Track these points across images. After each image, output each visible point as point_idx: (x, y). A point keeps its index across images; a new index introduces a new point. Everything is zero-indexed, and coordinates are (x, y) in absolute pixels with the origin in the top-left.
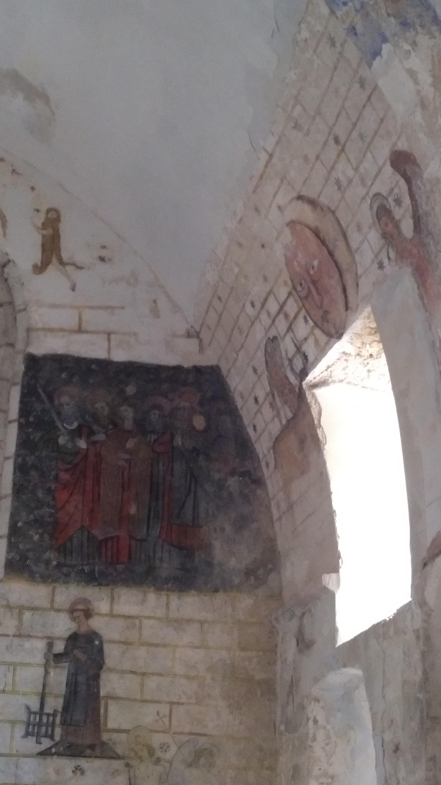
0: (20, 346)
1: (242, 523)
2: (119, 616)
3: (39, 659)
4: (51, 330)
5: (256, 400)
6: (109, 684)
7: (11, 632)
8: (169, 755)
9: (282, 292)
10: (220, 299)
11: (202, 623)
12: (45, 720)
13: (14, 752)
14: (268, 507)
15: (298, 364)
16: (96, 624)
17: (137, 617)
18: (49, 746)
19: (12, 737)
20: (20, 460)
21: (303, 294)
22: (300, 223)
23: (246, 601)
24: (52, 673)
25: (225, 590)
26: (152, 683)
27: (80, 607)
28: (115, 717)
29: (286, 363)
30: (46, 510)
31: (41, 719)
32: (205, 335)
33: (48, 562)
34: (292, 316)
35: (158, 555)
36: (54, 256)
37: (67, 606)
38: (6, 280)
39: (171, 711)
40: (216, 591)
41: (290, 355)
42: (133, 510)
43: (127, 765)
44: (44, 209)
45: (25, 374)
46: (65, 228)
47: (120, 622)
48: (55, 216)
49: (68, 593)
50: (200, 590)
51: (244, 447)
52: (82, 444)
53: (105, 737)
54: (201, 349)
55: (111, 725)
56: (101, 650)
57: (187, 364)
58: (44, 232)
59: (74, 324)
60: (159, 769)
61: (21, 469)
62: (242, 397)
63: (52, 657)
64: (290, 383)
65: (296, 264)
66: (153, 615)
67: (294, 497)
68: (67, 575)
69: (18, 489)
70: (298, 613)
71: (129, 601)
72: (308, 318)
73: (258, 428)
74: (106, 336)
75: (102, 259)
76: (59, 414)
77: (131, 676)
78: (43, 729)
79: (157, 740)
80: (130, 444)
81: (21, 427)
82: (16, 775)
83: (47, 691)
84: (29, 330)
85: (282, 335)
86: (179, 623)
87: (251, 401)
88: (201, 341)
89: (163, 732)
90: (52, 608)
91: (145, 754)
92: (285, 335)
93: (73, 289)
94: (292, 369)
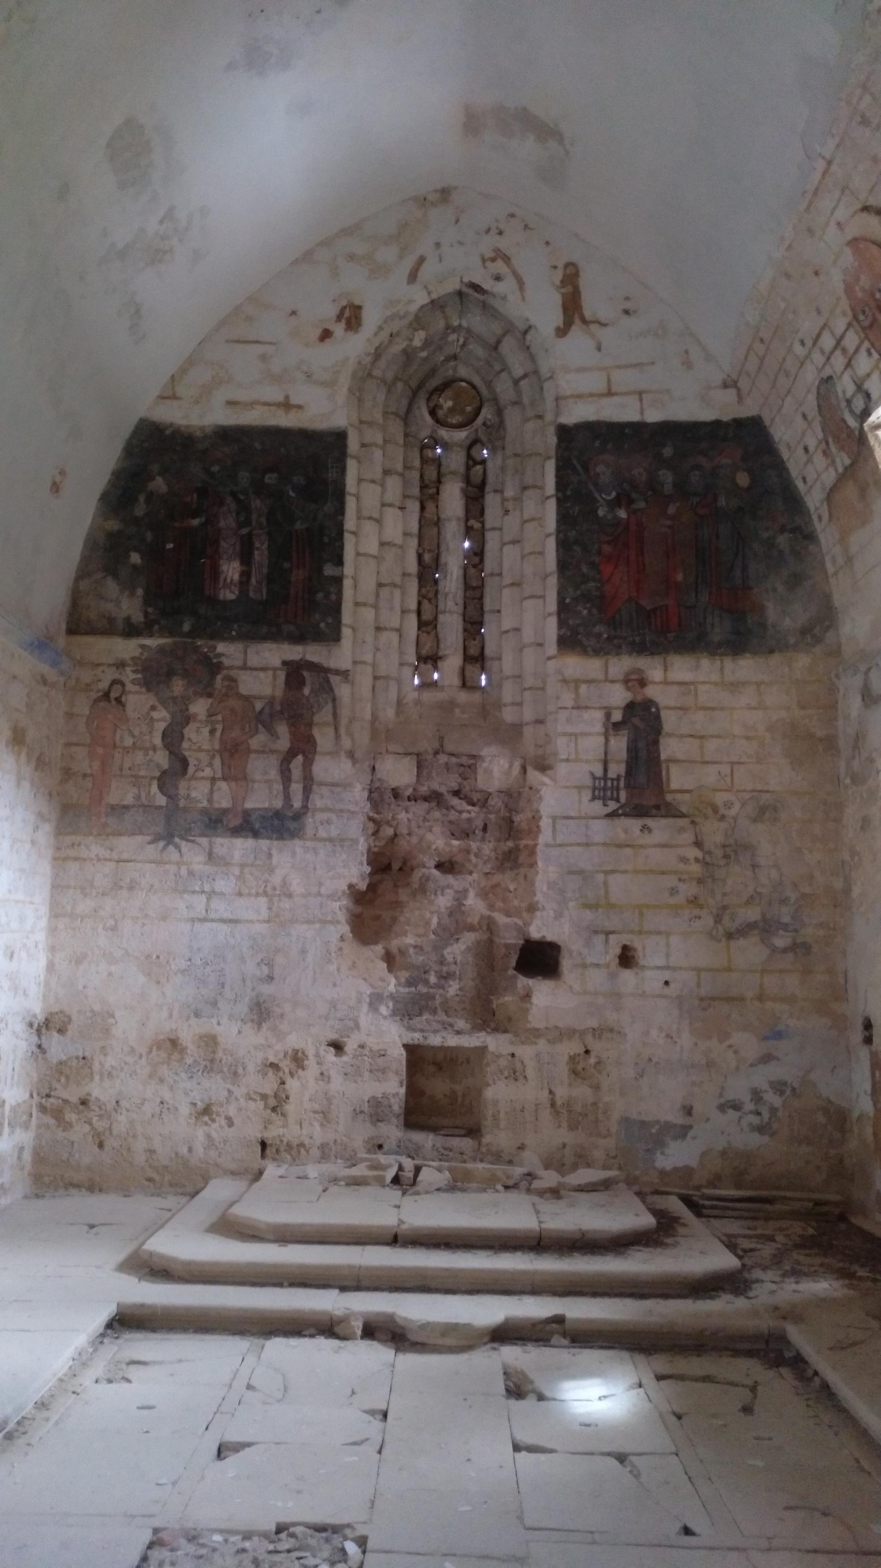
0: (549, 417)
1: (796, 580)
2: (673, 683)
3: (599, 728)
4: (580, 396)
5: (806, 449)
6: (669, 748)
7: (570, 704)
8: (733, 812)
9: (840, 325)
10: (762, 341)
11: (758, 684)
12: (609, 784)
13: (583, 815)
14: (823, 563)
15: (859, 404)
16: (651, 692)
17: (692, 683)
18: (616, 808)
19: (580, 802)
20: (561, 535)
21: (867, 323)
22: (865, 239)
23: (802, 661)
24: (612, 741)
25: (781, 651)
26: (711, 745)
27: (634, 677)
28: (677, 779)
29: (843, 404)
30: (592, 585)
31: (605, 784)
32: (744, 384)
33: (599, 635)
34: (851, 351)
35: (709, 620)
36: (576, 315)
37: (621, 677)
38: (528, 348)
39: (732, 770)
40: (771, 652)
41: (849, 394)
42: (680, 577)
43: (693, 822)
44: (561, 265)
45: (558, 446)
46: (584, 282)
48: (574, 271)
49: (622, 664)
50: (755, 653)
51: (794, 502)
52: (622, 514)
53: (669, 797)
55: (674, 786)
56: (658, 717)
57: (725, 419)
58: (563, 290)
59: (602, 387)
60: (724, 825)
61: (563, 545)
62: (789, 448)
63: (611, 725)
64: (848, 427)
65: (857, 288)
66: (707, 680)
67: (854, 549)
68: (619, 647)
69: (562, 566)
70: (863, 668)
71: (682, 668)
72: (873, 351)
73: (808, 479)
74: (637, 396)
75: (627, 312)
76: (596, 485)
77: (691, 739)
78: (609, 793)
79: (720, 798)
80: (672, 510)
81: (559, 502)
82: (587, 836)
83: (609, 758)
84: (557, 399)
85: (839, 372)
86: (735, 687)
87: (800, 451)
88: (739, 390)
89: (726, 790)
90: (606, 680)
91: (709, 811)
92: (843, 373)
93: (599, 349)
94: (852, 412)
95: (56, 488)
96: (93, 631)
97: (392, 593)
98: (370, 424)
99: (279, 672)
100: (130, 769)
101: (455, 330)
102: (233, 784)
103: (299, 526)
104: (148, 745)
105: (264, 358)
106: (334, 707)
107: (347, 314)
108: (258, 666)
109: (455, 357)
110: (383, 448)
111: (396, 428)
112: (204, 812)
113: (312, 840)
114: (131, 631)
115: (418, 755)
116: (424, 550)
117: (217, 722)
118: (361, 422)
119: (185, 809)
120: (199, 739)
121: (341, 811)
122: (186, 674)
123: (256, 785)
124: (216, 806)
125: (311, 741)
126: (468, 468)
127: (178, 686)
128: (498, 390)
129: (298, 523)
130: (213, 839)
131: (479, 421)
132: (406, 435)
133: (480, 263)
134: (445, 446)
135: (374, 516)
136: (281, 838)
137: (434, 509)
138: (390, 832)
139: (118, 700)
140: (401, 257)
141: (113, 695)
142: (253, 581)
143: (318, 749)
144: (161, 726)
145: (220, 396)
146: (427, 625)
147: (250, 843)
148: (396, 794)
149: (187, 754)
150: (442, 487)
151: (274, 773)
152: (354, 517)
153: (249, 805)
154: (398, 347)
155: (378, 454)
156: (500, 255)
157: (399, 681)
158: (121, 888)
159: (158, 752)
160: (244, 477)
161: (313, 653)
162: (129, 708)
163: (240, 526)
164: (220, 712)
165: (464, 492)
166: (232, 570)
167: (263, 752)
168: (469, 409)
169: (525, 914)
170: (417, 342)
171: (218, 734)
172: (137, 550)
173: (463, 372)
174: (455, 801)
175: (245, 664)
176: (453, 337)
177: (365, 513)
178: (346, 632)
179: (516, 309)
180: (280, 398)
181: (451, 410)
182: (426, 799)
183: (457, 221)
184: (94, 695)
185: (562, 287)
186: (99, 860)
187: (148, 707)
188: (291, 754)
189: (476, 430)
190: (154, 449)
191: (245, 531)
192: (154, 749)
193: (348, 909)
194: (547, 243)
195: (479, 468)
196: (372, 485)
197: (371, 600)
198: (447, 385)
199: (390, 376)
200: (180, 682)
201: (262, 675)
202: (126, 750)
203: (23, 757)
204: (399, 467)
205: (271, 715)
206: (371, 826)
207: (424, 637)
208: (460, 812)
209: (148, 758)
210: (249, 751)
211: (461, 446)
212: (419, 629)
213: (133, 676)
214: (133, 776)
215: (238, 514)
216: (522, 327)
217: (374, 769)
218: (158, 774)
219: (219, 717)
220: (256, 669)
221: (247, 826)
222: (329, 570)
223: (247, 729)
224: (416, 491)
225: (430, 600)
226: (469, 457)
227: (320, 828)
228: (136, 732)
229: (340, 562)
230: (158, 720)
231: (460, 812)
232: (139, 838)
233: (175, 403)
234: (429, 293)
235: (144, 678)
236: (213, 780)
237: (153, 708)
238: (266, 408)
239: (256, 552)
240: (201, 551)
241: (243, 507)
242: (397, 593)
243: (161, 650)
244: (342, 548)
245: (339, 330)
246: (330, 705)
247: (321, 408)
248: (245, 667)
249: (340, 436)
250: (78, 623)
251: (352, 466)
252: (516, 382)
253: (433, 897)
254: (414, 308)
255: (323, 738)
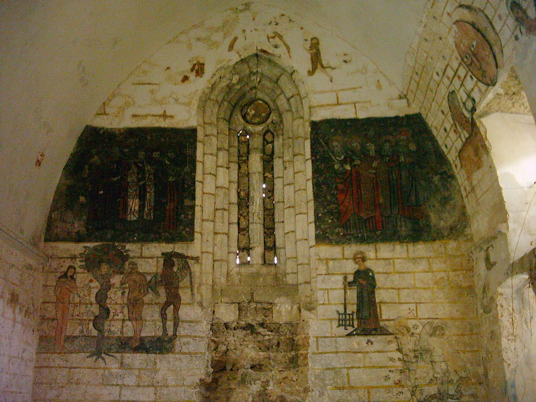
0: (306, 117)
1: (445, 201)
2: (381, 259)
3: (340, 285)
4: (322, 106)
5: (445, 130)
6: (380, 295)
7: (324, 272)
8: (418, 331)
9: (455, 64)
10: (417, 73)
11: (428, 258)
12: (348, 317)
13: (334, 335)
14: (459, 191)
15: (470, 105)
16: (369, 264)
17: (391, 259)
18: (352, 331)
19: (332, 328)
20: (315, 180)
21: (469, 63)
22: (462, 21)
23: (452, 245)
24: (348, 292)
25: (440, 240)
26: (404, 293)
27: (359, 256)
28: (386, 313)
29: (462, 105)
30: (332, 206)
31: (346, 317)
32: (410, 96)
33: (338, 234)
34: (462, 77)
35: (399, 224)
36: (319, 64)
37: (352, 257)
38: (294, 82)
39: (416, 307)
40: (434, 240)
41: (464, 100)
42: (381, 201)
43: (396, 338)
44: (309, 39)
45: (311, 132)
46: (322, 47)
47: (383, 262)
48: (316, 42)
49: (351, 249)
50: (425, 241)
51: (441, 158)
52: (348, 167)
53: (382, 324)
54: (409, 105)
55: (384, 317)
56: (373, 278)
58: (311, 52)
59: (335, 101)
60: (413, 338)
61: (316, 185)
63: (347, 284)
64: (465, 117)
65: (462, 45)
66: (400, 256)
67: (475, 182)
68: (350, 240)
69: (316, 196)
70: (485, 247)
71: (385, 250)
72: (473, 77)
73: (448, 146)
74: (353, 105)
75: (345, 62)
76: (333, 152)
77: (392, 290)
78: (348, 322)
79: (411, 323)
80: (375, 164)
81: (313, 162)
82: (336, 347)
83: (347, 302)
84: (310, 108)
85: (458, 89)
86: (415, 260)
87: (442, 131)
88: (408, 100)
89: (414, 319)
90: (344, 258)
91: (405, 331)
92: (460, 89)
93: (331, 81)
94: (466, 108)
95: (39, 163)
96: (58, 239)
97: (223, 214)
98: (210, 124)
99: (160, 259)
100: (78, 315)
101: (254, 74)
102: (134, 323)
103: (171, 179)
104: (88, 302)
105: (152, 92)
106: (191, 278)
107: (196, 67)
108: (148, 256)
109: (255, 88)
110: (217, 137)
111: (224, 126)
112: (119, 338)
113: (178, 353)
114: (79, 239)
115: (239, 303)
116: (241, 190)
117: (126, 288)
118: (205, 123)
119: (108, 338)
120: (116, 298)
121: (195, 337)
122: (109, 262)
123: (147, 323)
124: (125, 335)
125: (177, 297)
126: (264, 146)
127: (105, 268)
128: (279, 104)
129: (171, 178)
130: (124, 355)
131: (269, 120)
132: (230, 129)
133: (267, 39)
134: (251, 134)
135: (213, 173)
136: (161, 353)
137: (246, 168)
138: (224, 348)
139: (72, 277)
140: (225, 38)
141: (69, 275)
142: (146, 209)
143: (182, 302)
144: (95, 291)
145: (129, 112)
146: (243, 230)
147: (144, 356)
148: (227, 326)
149: (109, 306)
150: (250, 157)
151: (157, 316)
152: (201, 174)
153: (143, 334)
154: (224, 83)
155: (214, 139)
156: (277, 35)
157: (228, 262)
158: (72, 383)
159: (93, 306)
160: (141, 154)
161: (179, 248)
162: (78, 280)
163: (139, 180)
164: (127, 282)
165: (262, 159)
166: (134, 204)
167: (152, 304)
168: (264, 114)
169: (302, 394)
170: (234, 81)
171: (126, 294)
172: (83, 195)
173: (260, 95)
174: (261, 330)
175: (141, 255)
176: (253, 78)
177: (207, 171)
178: (197, 236)
179: (285, 61)
180: (161, 112)
181: (254, 116)
182: (244, 329)
183: (254, 19)
184: (59, 275)
185: (311, 50)
186: (60, 367)
187: (88, 280)
188: (167, 304)
189: (268, 126)
190: (93, 140)
191: (142, 183)
192: (91, 304)
193: (200, 393)
194: (302, 28)
195: (270, 145)
196: (211, 157)
197: (211, 218)
198: (252, 102)
199: (220, 98)
200: (106, 267)
201: (151, 261)
202: (76, 305)
203: (17, 311)
204: (226, 146)
205: (156, 283)
206: (213, 345)
207: (241, 237)
208: (264, 336)
209: (88, 309)
210: (143, 303)
211: (260, 135)
212: (239, 233)
213: (80, 264)
214: (80, 320)
215: (138, 174)
216: (290, 71)
217: (214, 312)
218: (93, 318)
219: (127, 285)
220: (147, 258)
221: (143, 346)
222: (187, 202)
223: (142, 292)
224: (236, 159)
225: (244, 217)
226: (264, 139)
227: (184, 347)
228: (81, 295)
229: (194, 198)
230: (94, 288)
231: (264, 336)
232: (83, 355)
233: (105, 117)
234: (240, 56)
235: (86, 264)
236: (124, 320)
237: (91, 281)
238: (154, 118)
239: (148, 194)
240: (119, 194)
241: (141, 170)
242: (226, 213)
243: (95, 249)
244: (194, 190)
245: (192, 76)
246: (188, 276)
247: (184, 117)
248: (141, 257)
249: (193, 131)
250: (51, 234)
251: (199, 146)
252: (288, 100)
253: (249, 385)
254: (232, 63)
255: (185, 295)
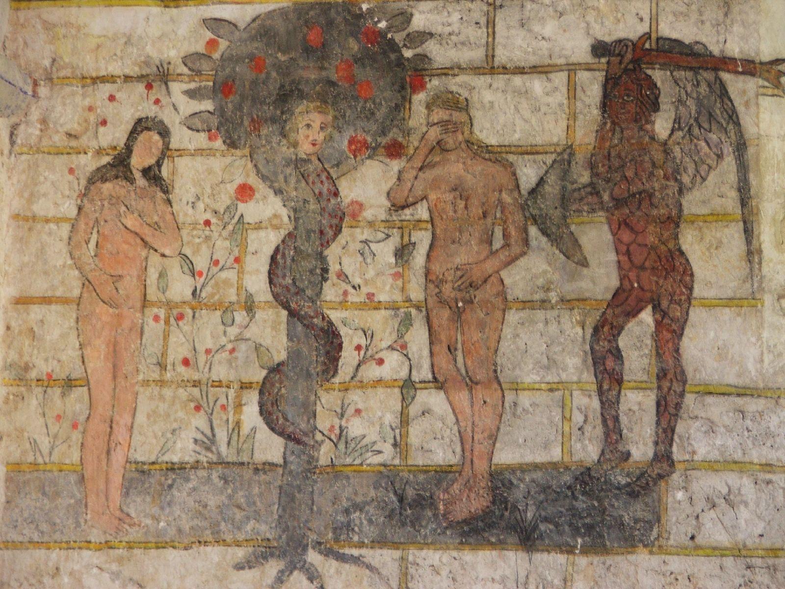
99: (583, 76)
100: (186, 362)
102: (462, 397)
104: (232, 295)
106: (743, 168)
112: (387, 476)
113: (681, 551)
119: (335, 472)
120: (367, 276)
122: (328, 95)
123: (525, 399)
124: (419, 460)
125: (674, 266)
127: (309, 127)
130: (413, 554)
136: (597, 546)
139: (152, 174)
141: (138, 161)
143: (696, 292)
144: (265, 242)
149: (335, 316)
151: (574, 365)
153: (505, 456)
159: (259, 315)
164: (425, 198)
167: (544, 304)
171: (419, 258)
175: (490, 56)
184: (88, 163)
187: (231, 188)
188: (624, 303)
192: (250, 307)
200: (317, 119)
201: (537, 85)
202: (176, 314)
205: (564, 200)
210: (505, 302)
213: (188, 106)
214: (196, 384)
218: (259, 375)
219: (422, 212)
220: (520, 71)
221: (504, 515)
223: (498, 243)
228: (201, 263)
230: (258, 226)
232: (214, 553)
235: (220, 111)
236: (408, 387)
237: (245, 192)
246: (730, 162)
248: (490, 67)
255: (712, 260)
